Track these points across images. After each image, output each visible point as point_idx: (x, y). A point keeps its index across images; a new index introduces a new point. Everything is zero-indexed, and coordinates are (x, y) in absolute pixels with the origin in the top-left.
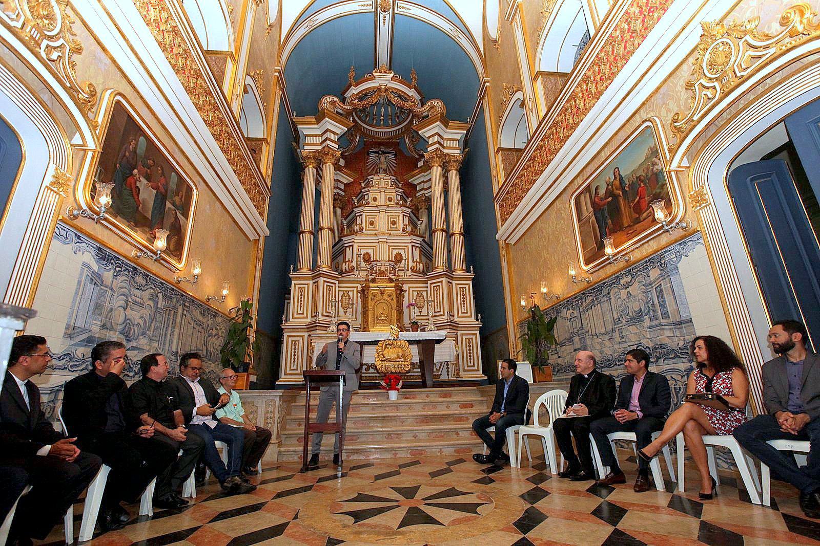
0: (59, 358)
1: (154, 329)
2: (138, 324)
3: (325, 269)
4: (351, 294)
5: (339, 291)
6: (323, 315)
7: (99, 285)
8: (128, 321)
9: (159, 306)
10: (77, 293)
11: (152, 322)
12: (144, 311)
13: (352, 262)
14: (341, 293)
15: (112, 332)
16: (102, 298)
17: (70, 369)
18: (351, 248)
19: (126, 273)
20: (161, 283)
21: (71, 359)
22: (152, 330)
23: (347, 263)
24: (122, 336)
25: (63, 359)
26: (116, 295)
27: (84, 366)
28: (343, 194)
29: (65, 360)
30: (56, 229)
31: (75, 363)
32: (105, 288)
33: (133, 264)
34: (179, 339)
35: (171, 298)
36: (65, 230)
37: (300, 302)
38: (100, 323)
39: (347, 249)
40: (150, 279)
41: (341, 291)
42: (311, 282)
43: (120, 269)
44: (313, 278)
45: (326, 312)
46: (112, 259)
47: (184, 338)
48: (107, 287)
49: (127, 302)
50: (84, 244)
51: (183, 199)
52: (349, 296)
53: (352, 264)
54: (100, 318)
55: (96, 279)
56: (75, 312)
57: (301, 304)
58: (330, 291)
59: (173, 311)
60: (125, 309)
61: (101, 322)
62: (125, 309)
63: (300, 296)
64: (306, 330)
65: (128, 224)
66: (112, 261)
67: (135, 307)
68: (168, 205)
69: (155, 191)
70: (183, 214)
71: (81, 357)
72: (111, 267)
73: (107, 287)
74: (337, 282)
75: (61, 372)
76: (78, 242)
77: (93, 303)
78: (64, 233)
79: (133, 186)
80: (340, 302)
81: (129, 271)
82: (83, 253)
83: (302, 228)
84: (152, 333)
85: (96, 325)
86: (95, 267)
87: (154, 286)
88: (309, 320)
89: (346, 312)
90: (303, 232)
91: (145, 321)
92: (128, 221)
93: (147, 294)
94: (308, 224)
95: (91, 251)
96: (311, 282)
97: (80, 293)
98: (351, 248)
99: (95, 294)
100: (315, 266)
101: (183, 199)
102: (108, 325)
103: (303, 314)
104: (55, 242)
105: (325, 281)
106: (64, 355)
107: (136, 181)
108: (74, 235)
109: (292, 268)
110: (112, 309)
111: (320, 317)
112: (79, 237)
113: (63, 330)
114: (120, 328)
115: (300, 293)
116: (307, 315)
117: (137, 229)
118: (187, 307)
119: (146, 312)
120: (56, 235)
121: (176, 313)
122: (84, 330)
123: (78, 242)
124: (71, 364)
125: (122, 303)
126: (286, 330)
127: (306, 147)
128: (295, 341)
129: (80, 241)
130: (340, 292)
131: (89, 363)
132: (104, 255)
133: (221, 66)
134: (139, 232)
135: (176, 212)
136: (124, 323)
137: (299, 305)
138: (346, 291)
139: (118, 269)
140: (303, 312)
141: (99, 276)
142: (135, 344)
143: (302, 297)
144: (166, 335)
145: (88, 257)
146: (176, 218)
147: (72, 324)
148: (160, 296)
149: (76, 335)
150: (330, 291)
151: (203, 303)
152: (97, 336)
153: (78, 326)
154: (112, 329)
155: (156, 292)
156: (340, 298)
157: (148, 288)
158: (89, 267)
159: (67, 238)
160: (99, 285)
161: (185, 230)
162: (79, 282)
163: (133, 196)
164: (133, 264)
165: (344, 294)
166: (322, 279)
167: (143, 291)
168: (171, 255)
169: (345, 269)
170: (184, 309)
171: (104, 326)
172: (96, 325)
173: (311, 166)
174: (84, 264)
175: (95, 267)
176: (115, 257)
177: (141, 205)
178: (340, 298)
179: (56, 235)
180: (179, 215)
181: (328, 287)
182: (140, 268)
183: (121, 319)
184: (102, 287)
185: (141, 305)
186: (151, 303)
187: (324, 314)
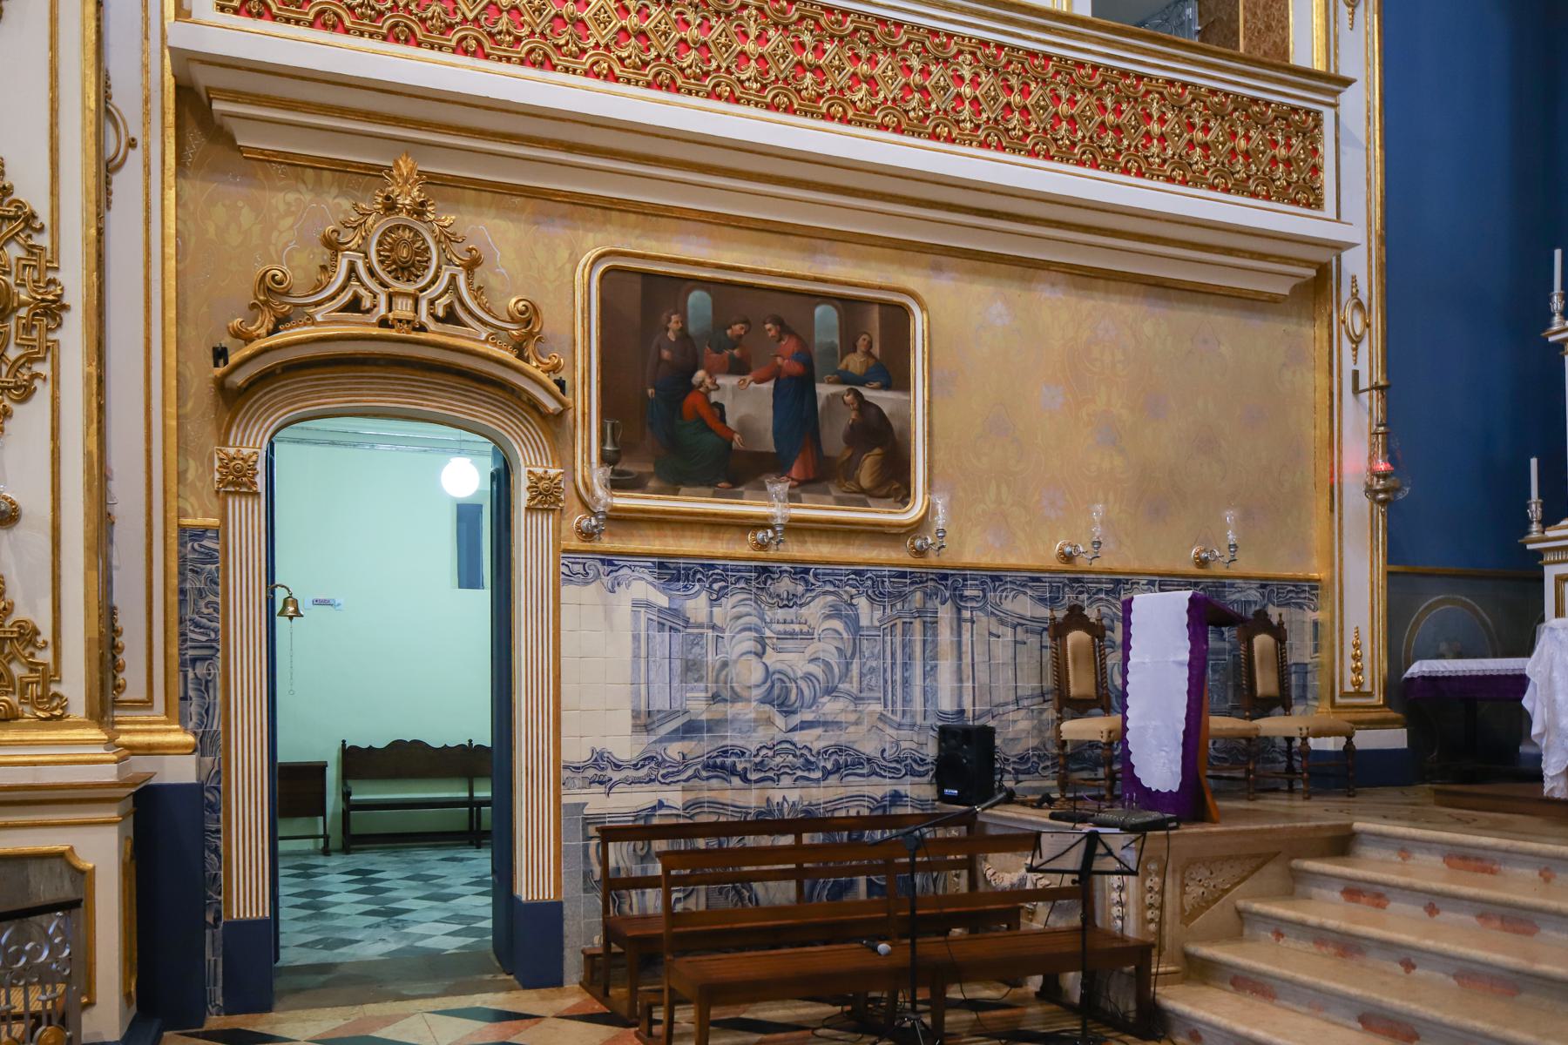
0: (635, 765)
1: (861, 675)
2: (808, 677)
7: (681, 628)
8: (776, 676)
9: (864, 622)
10: (636, 656)
11: (848, 665)
12: (813, 648)
15: (739, 706)
16: (697, 650)
17: (663, 781)
19: (742, 584)
20: (856, 573)
21: (659, 765)
22: (856, 679)
24: (767, 707)
25: (643, 766)
26: (727, 634)
27: (690, 772)
29: (647, 767)
30: (564, 569)
31: (670, 770)
32: (696, 631)
33: (753, 564)
34: (960, 680)
35: (902, 596)
36: (578, 563)
38: (703, 694)
40: (815, 575)
43: (723, 584)
46: (695, 573)
47: (982, 676)
48: (701, 626)
49: (761, 641)
50: (625, 571)
51: (876, 350)
54: (702, 685)
55: (671, 620)
56: (643, 688)
60: (760, 655)
61: (707, 692)
62: (760, 655)
65: (710, 491)
66: (699, 576)
67: (789, 644)
68: (823, 390)
69: (769, 386)
70: (886, 387)
71: (678, 758)
72: (697, 586)
73: (702, 627)
75: (647, 787)
76: (612, 571)
77: (677, 664)
78: (578, 568)
79: (704, 411)
81: (748, 581)
82: (628, 586)
84: (855, 685)
85: (696, 699)
86: (662, 601)
87: (835, 586)
91: (827, 664)
92: (709, 485)
93: (814, 610)
95: (645, 576)
97: (643, 653)
99: (676, 648)
101: (876, 350)
102: (727, 694)
104: (567, 591)
106: (645, 759)
107: (706, 395)
108: (599, 564)
110: (725, 664)
112: (610, 563)
113: (627, 721)
114: (757, 693)
117: (740, 489)
118: (973, 599)
119: (827, 649)
120: (570, 577)
121: (931, 626)
122: (671, 715)
123: (612, 571)
124: (663, 772)
125: (750, 645)
126: (1549, 557)
129: (616, 568)
131: (699, 767)
132: (671, 571)
134: (747, 493)
135: (858, 395)
136: (765, 682)
139: (716, 586)
141: (674, 612)
142: (808, 716)
144: (906, 682)
145: (643, 587)
146: (863, 405)
147: (643, 707)
148: (862, 603)
149: (657, 724)
152: (704, 717)
153: (656, 708)
154: (736, 698)
155: (846, 597)
157: (814, 598)
158: (648, 605)
159: (587, 573)
160: (681, 628)
161: (907, 421)
162: (636, 638)
163: (709, 429)
164: (753, 564)
167: (801, 606)
168: (870, 501)
170: (959, 610)
171: (715, 698)
172: (696, 699)
174: (636, 604)
175: (662, 601)
176: (703, 565)
177: (737, 437)
179: (563, 578)
180: (869, 394)
182: (776, 565)
183: (757, 675)
184: (689, 630)
185: (808, 636)
186: (837, 624)
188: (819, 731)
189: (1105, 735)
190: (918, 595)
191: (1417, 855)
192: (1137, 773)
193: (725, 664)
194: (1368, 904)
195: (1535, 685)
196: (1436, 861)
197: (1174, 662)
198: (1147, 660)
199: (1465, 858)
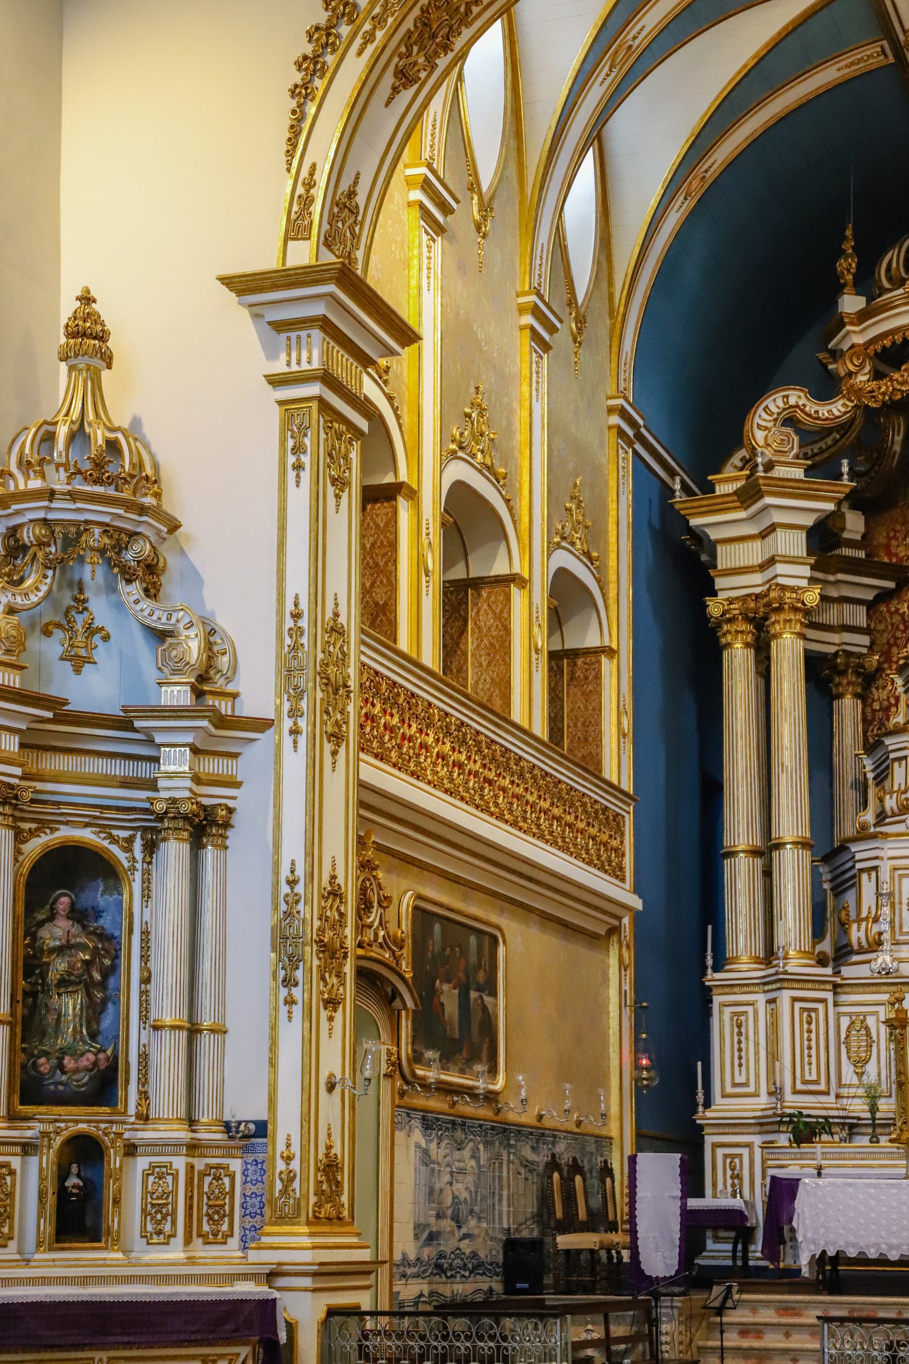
3: (795, 965)
4: (871, 1021)
5: (838, 1016)
6: (796, 1092)
13: (876, 920)
14: (845, 1022)
18: (874, 874)
23: (864, 924)
28: (865, 640)
37: (736, 1055)
39: (864, 876)
41: (845, 1014)
42: (761, 999)
44: (765, 984)
45: (805, 1082)
52: (867, 1029)
53: (876, 929)
57: (740, 1058)
58: (809, 1023)
59: (497, 1162)
63: (736, 1038)
64: (757, 1129)
74: (829, 996)
80: (843, 1047)
83: (727, 842)
88: (763, 1100)
89: (860, 1075)
90: (732, 854)
94: (742, 829)
96: (761, 999)
98: (874, 874)
100: (769, 955)
103: (746, 1085)
105: (794, 1000)
109: (710, 962)
111: (789, 1097)
115: (736, 1030)
116: (757, 1083)
127: (720, 583)
128: (733, 1156)
130: (842, 1018)
133: (501, 611)
137: (736, 1062)
138: (858, 1014)
140: (748, 1079)
143: (743, 1038)
144: (494, 1205)
148: (481, 1147)
150: (809, 1023)
151: (532, 1127)
156: (843, 1036)
161: (496, 1016)
165: (853, 1023)
166: (785, 996)
169: (860, 944)
170: (509, 1153)
173: (738, 645)
178: (843, 1036)
181: (805, 1014)
187: (799, 1086)
188: (467, 1241)
189: (598, 1244)
190: (497, 1143)
191: (762, 1311)
192: (643, 1266)
193: (441, 1191)
194: (753, 1337)
195: (799, 1214)
196: (771, 1312)
197: (669, 1197)
198: (649, 1195)
199: (787, 1309)
